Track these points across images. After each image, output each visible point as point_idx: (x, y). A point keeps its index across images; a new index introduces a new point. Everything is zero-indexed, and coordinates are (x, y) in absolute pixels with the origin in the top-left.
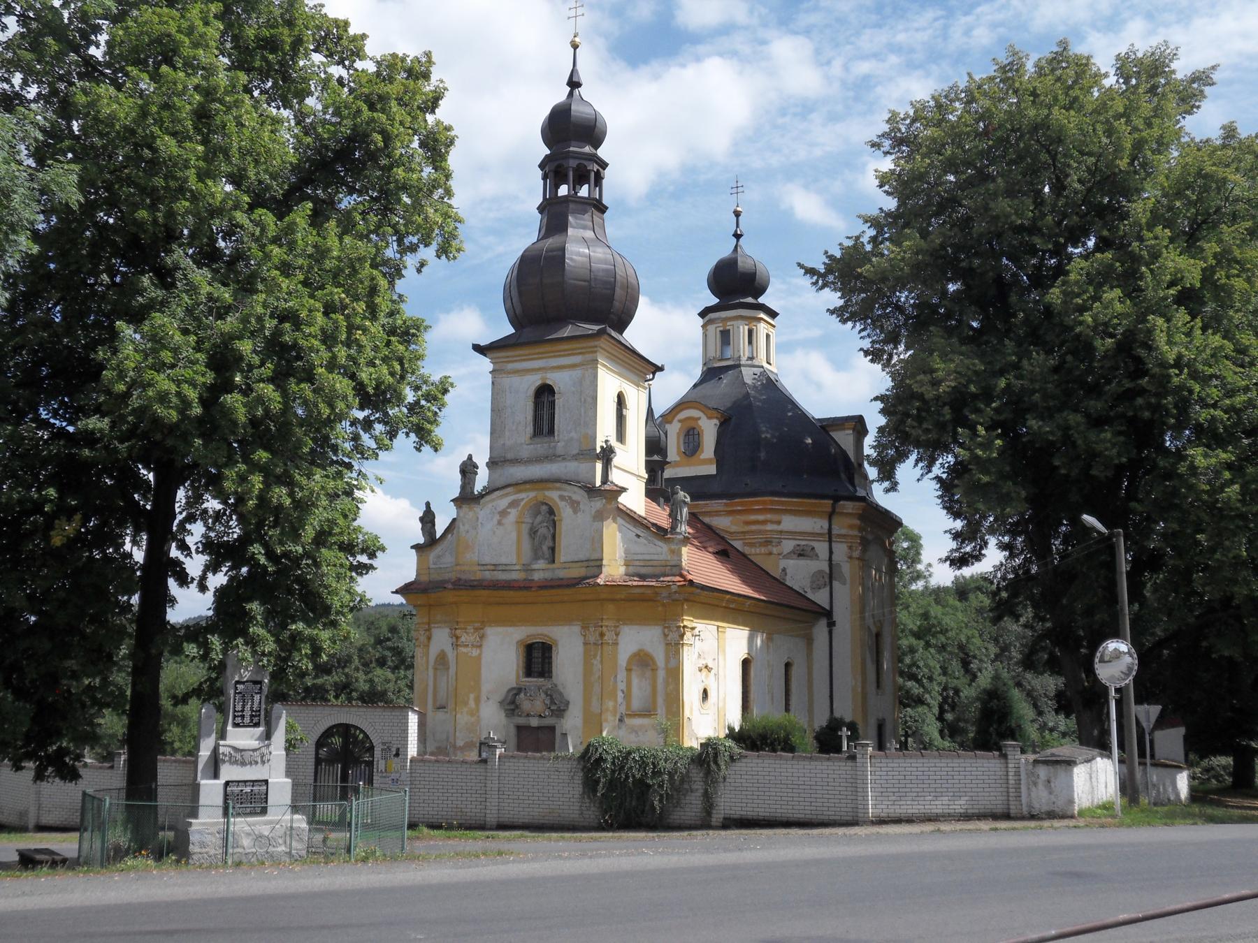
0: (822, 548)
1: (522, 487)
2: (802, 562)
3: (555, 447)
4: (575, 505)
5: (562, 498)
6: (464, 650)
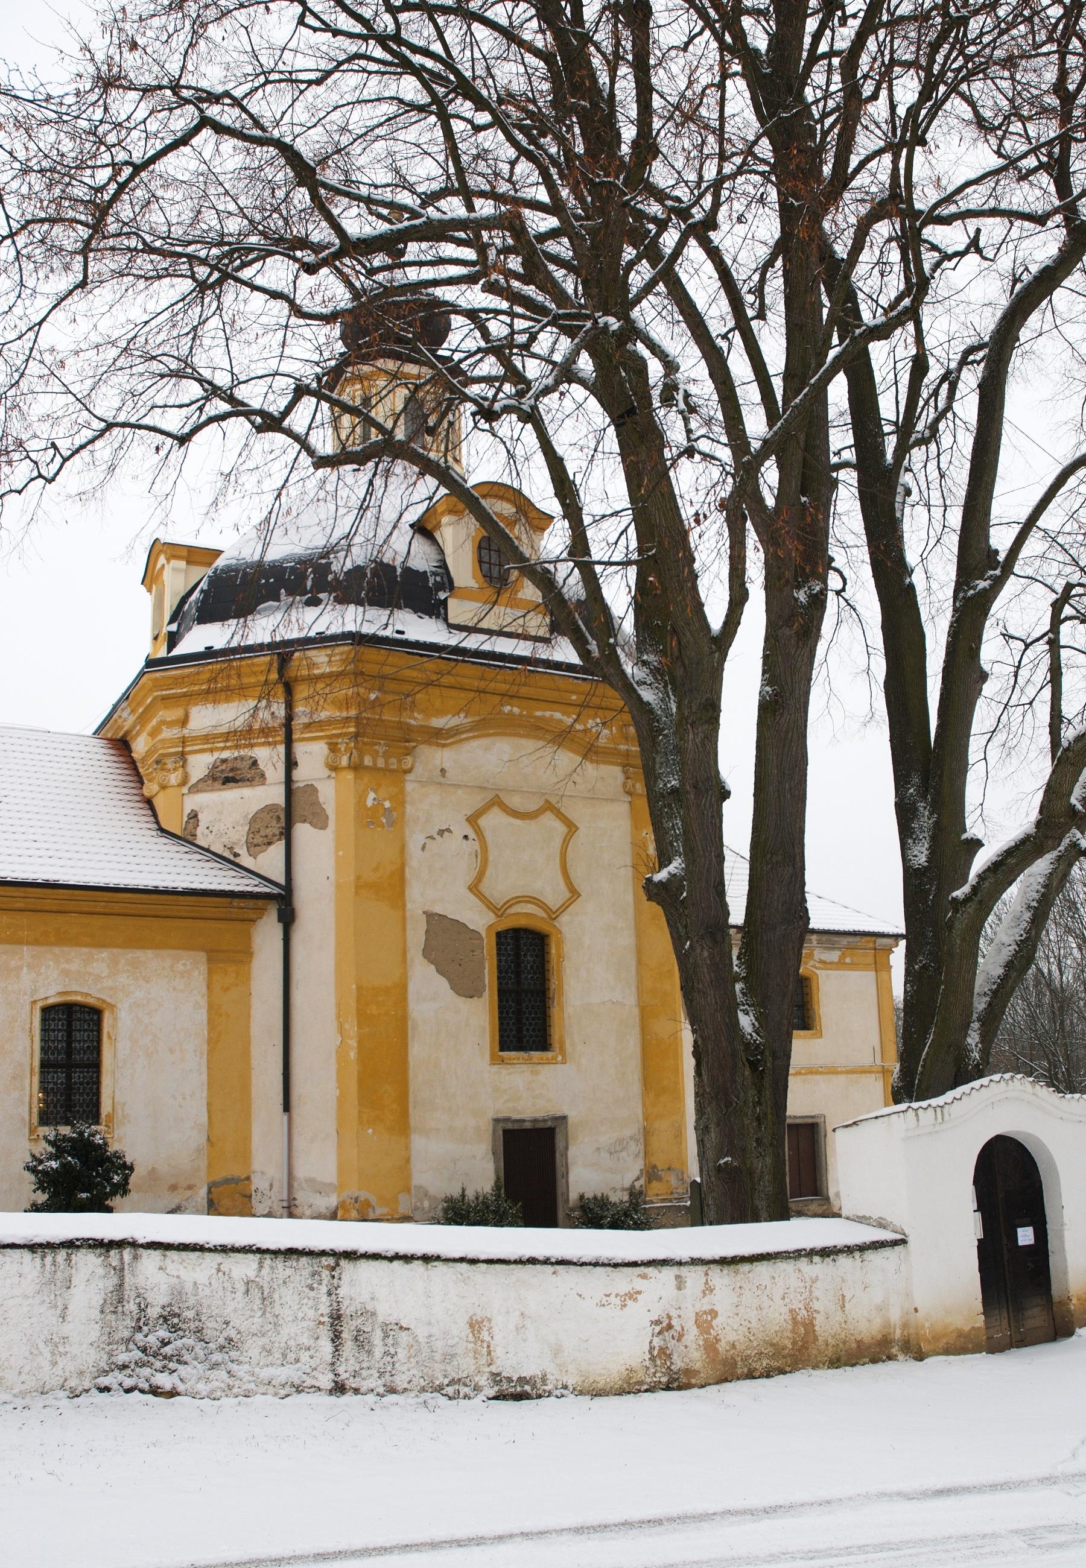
0: (269, 758)
2: (231, 795)
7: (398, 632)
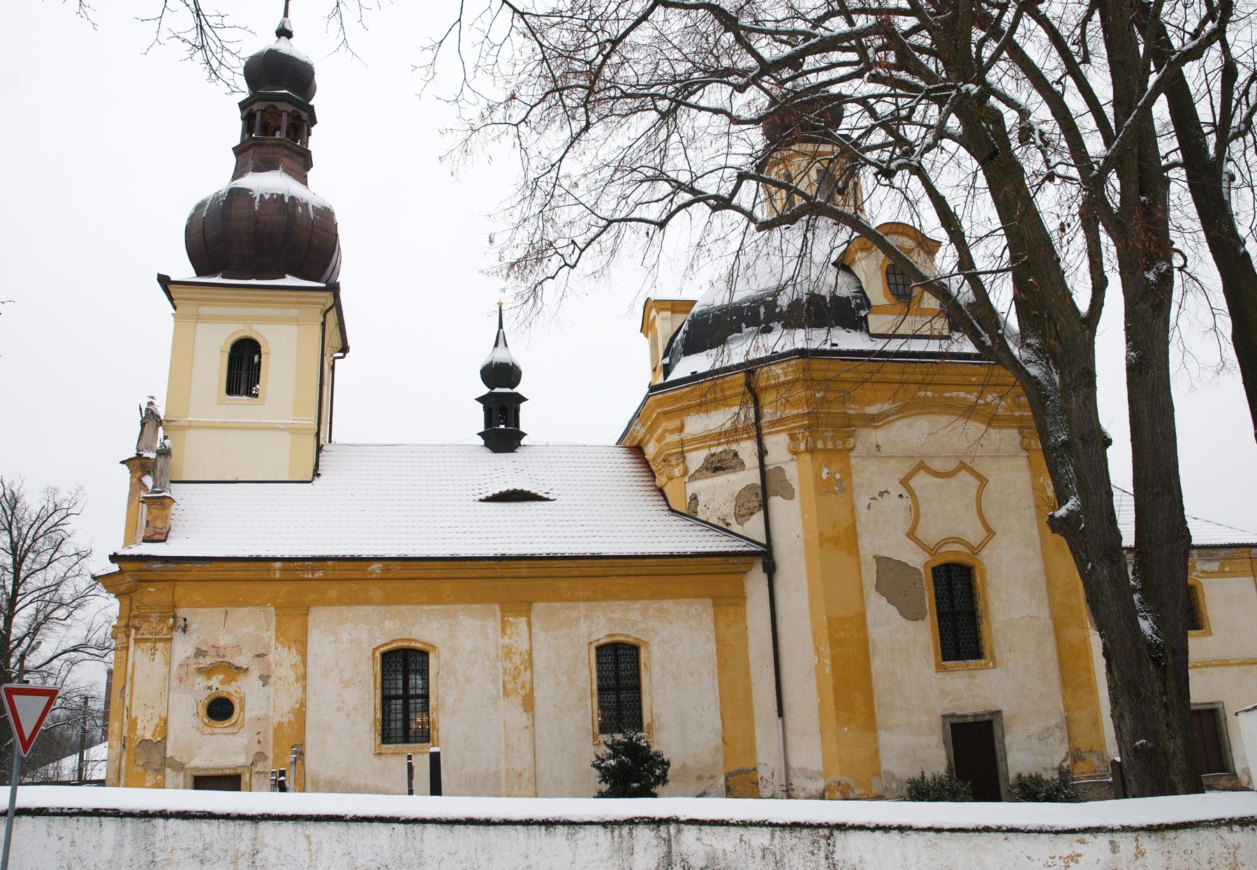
0: (747, 450)
2: (720, 480)
7: (833, 345)
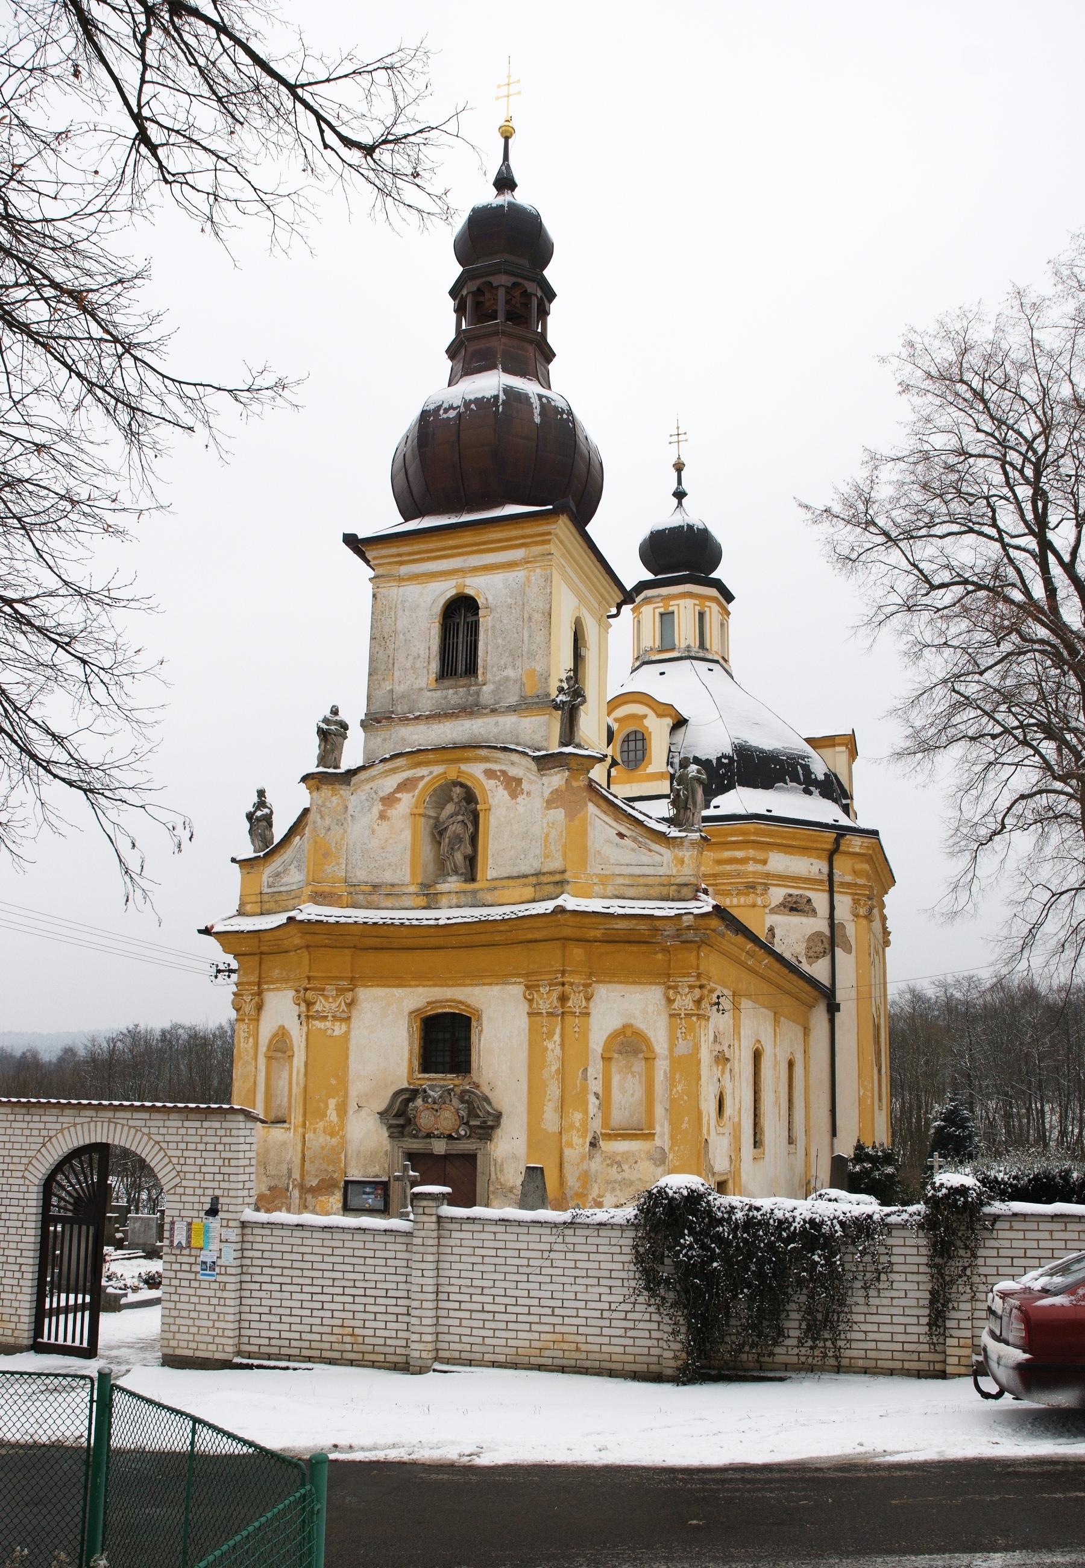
0: (820, 900)
1: (421, 757)
2: (795, 920)
3: (478, 693)
4: (513, 785)
5: (490, 774)
6: (318, 1024)
